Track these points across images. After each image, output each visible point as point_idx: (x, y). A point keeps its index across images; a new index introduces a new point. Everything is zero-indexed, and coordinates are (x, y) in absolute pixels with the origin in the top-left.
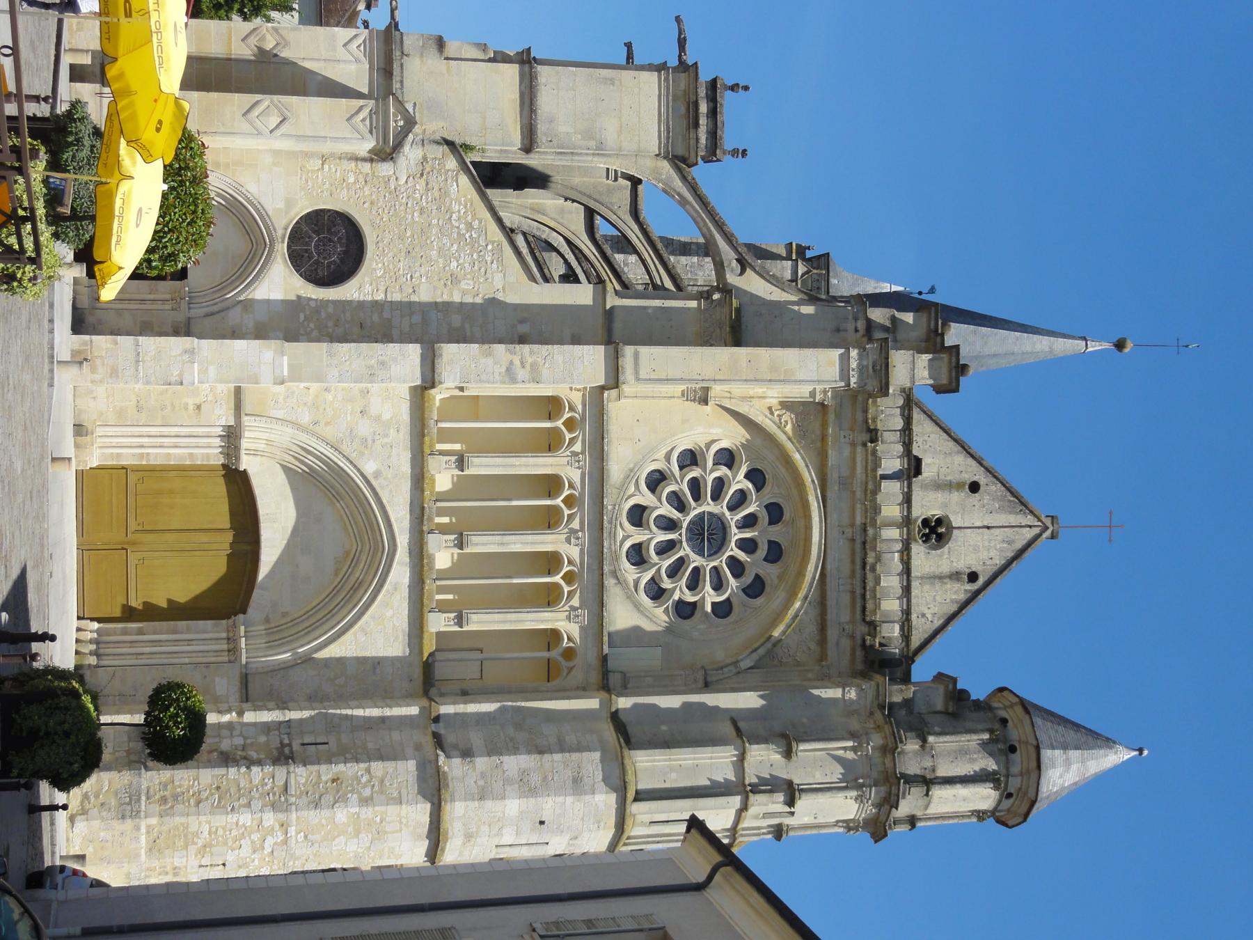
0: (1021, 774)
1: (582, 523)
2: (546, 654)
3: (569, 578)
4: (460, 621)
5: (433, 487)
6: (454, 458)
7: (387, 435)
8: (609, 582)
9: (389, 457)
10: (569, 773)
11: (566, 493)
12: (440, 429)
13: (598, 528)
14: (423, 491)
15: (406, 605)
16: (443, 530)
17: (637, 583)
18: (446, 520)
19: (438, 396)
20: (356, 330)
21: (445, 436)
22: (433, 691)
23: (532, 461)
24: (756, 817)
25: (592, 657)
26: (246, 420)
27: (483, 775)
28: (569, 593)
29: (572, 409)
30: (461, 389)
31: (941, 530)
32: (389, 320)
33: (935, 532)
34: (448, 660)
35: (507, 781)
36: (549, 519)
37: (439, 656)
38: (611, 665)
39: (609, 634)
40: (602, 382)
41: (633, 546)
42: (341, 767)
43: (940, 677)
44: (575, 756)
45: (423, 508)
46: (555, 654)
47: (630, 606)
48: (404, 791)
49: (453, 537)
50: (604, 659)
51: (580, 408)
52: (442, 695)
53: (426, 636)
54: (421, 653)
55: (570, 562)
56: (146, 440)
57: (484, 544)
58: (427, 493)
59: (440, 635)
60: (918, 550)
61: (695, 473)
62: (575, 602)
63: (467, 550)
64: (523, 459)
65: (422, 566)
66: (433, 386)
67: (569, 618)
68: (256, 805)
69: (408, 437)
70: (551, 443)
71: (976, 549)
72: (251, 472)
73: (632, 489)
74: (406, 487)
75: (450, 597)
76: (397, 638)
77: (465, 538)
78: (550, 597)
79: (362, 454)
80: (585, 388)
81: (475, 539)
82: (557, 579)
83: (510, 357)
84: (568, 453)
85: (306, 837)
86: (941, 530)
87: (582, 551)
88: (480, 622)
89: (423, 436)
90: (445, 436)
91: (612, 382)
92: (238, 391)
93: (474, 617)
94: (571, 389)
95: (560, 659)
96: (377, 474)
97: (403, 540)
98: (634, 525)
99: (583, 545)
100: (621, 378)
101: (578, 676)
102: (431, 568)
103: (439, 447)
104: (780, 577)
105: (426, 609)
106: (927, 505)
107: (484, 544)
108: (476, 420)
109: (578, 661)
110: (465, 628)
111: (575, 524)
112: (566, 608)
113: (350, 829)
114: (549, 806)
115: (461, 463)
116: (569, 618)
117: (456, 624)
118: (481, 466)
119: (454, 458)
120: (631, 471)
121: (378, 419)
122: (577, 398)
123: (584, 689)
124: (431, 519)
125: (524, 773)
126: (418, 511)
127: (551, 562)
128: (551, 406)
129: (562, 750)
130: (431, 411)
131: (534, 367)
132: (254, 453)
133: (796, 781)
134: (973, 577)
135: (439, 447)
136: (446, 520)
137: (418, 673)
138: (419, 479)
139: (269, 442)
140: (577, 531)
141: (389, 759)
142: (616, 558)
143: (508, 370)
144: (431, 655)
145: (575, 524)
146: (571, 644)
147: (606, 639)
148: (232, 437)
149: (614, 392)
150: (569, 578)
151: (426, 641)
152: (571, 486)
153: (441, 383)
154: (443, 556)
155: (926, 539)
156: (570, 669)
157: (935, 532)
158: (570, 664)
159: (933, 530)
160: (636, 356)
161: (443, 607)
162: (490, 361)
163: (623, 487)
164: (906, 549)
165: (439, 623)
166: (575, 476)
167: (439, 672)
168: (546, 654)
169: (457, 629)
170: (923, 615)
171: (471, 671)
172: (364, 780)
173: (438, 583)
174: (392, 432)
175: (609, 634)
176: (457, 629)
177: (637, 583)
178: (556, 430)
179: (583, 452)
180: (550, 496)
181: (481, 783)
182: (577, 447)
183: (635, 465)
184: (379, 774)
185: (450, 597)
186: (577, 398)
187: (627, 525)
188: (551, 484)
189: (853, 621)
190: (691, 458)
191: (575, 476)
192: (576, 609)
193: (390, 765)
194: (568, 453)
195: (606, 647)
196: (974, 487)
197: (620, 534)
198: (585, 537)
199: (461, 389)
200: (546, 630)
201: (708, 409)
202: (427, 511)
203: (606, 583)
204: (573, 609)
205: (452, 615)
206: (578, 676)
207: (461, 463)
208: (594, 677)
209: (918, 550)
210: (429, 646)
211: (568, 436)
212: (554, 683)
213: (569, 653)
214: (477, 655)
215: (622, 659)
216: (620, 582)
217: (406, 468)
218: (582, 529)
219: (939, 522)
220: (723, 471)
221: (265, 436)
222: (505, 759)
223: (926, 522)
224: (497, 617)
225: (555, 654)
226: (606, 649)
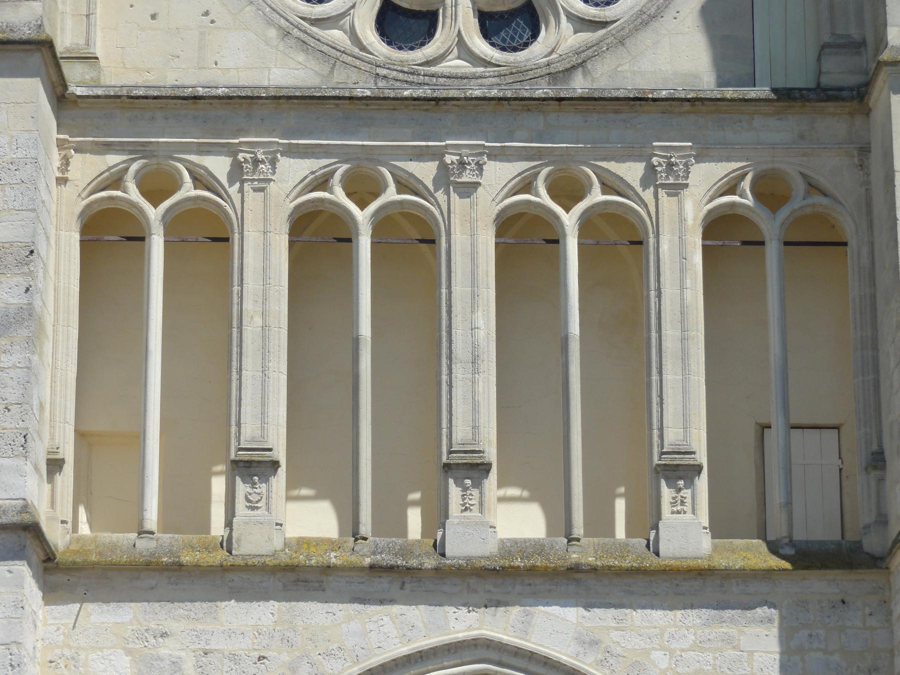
1: (420, 155)
2: (772, 250)
3: (568, 191)
4: (680, 472)
5: (319, 542)
6: (242, 488)
8: (579, 85)
9: (234, 657)
11: (339, 195)
12: (166, 525)
13: (435, 109)
14: (328, 569)
15: (637, 617)
16: (437, 516)
17: (583, 24)
18: (414, 519)
19: (67, 525)
21: (186, 507)
22: (872, 544)
23: (252, 284)
25: (779, 130)
28: (607, 188)
29: (116, 181)
30: (55, 465)
34: (788, 504)
36: (412, 242)
37: (777, 530)
38: (800, 79)
39: (719, 85)
40: (31, 90)
41: (486, 34)
45: (372, 567)
46: (771, 228)
47: (646, 38)
49: (455, 492)
50: (786, 96)
51: (113, 159)
52: (882, 520)
53: (721, 562)
54: (768, 574)
55: (527, 186)
57: (474, 411)
58: (334, 558)
59: (720, 527)
62: (631, 172)
63: (491, 454)
64: (248, 305)
65: (532, 571)
66: (33, 530)
67: (676, 189)
69: (181, 609)
70: (206, 237)
73: (336, 35)
74: (314, 614)
75: (620, 505)
76: (728, 641)
77: (456, 459)
78: (620, 243)
80: (61, 144)
81: (461, 433)
82: (570, 220)
84: (233, 190)
87: (496, 155)
88: (685, 416)
89: (178, 567)
90: (186, 507)
91: (36, 59)
93: (673, 436)
94: (62, 181)
95: (784, 212)
97: (461, 623)
98: (430, 34)
99: (480, 151)
100: (26, 33)
101: (831, 167)
102: (538, 547)
103: (218, 528)
105: (651, 561)
107: (474, 411)
108: (140, 437)
109: (790, 166)
110: (702, 458)
111: (425, 171)
112: (648, 195)
115: (253, 467)
116: (676, 189)
117: (690, 484)
118: (264, 413)
119: (242, 488)
120: (287, 34)
122: (88, 167)
123: (865, 150)
124: (407, 550)
126: (383, 583)
127: (524, 239)
128: (108, 236)
130: (113, 547)
135: (218, 528)
136: (414, 519)
137: (821, 585)
138: (296, 578)
140: (444, 168)
142: (519, 73)
144: (774, 549)
145: (425, 171)
146: (746, 184)
147: (730, 92)
149: (74, 73)
150: (568, 191)
151: (736, 562)
152: (322, 182)
153: (25, 508)
154: (513, 521)
156: (813, 187)
158: (800, 186)
161: (646, 519)
163: (331, 56)
165: (687, 530)
166: (293, 172)
167: (818, 526)
168: (772, 250)
169: (702, 483)
171: (817, 454)
173: (578, 530)
174: (167, 649)
175: (722, 82)
176: (702, 483)
177: (583, 24)
178: (171, 223)
179: (232, 151)
180: (348, 240)
182: (219, 166)
183: (270, 23)
185: (620, 505)
186: (88, 167)
187: (430, 50)
188: (316, 237)
191: (293, 172)
192: (651, 169)
194: (233, 190)
195: (752, 93)
197: (455, 64)
198: (457, 145)
199: (55, 465)
200: (707, 251)
202: (386, 559)
203: (579, 92)
204: (649, 178)
205: (667, 493)
206: (831, 167)
207: (253, 467)
208: (832, 124)
210: (752, 554)
211: (188, 190)
212: (848, 228)
213: (770, 191)
214: (775, 438)
215: (786, 50)
216: (580, 63)
217: (265, 613)
218: (437, 155)
224: (671, 376)
225: (771, 228)
226: (762, 91)
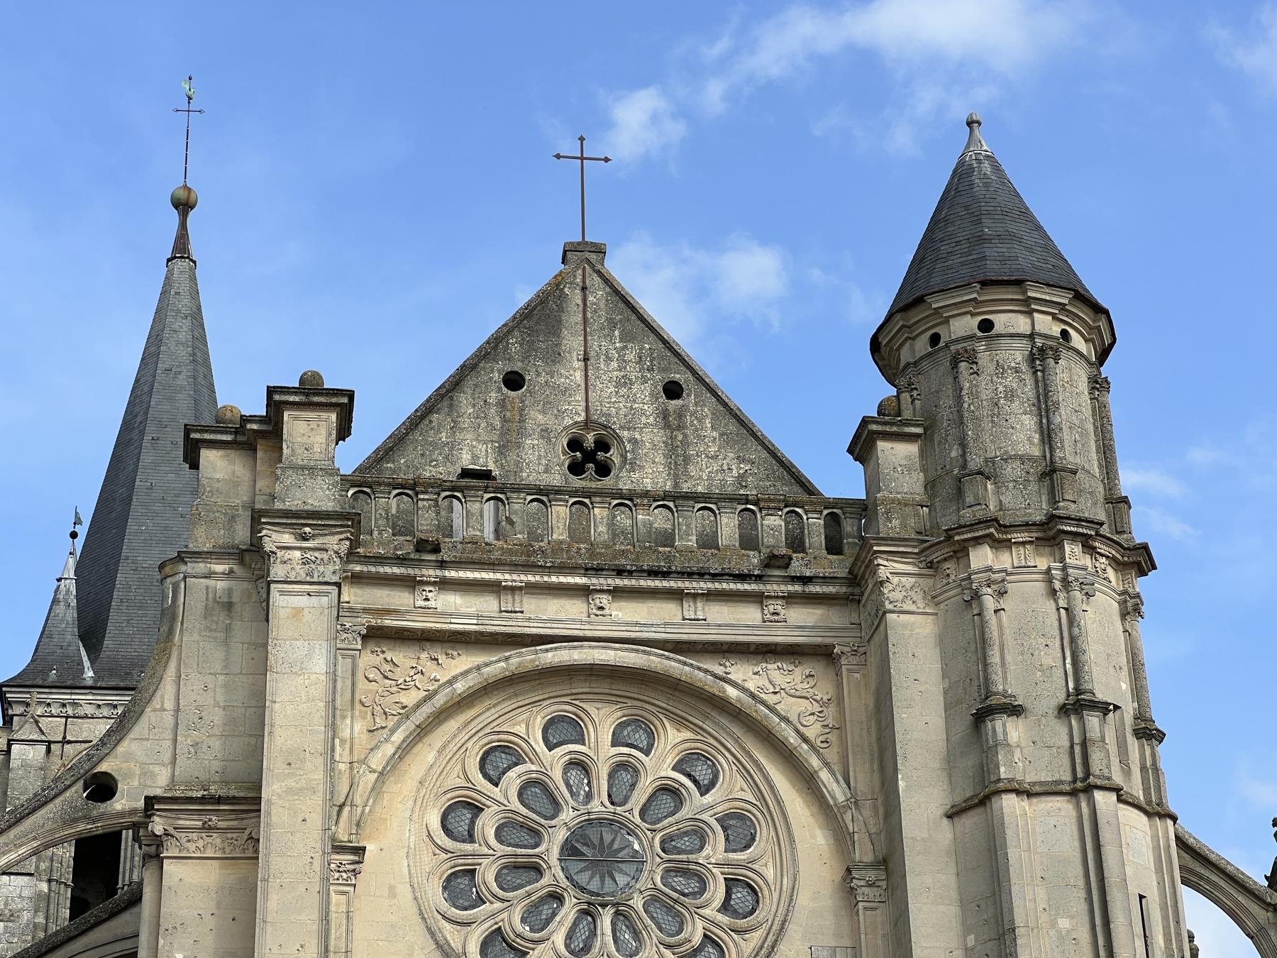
104: (681, 722)
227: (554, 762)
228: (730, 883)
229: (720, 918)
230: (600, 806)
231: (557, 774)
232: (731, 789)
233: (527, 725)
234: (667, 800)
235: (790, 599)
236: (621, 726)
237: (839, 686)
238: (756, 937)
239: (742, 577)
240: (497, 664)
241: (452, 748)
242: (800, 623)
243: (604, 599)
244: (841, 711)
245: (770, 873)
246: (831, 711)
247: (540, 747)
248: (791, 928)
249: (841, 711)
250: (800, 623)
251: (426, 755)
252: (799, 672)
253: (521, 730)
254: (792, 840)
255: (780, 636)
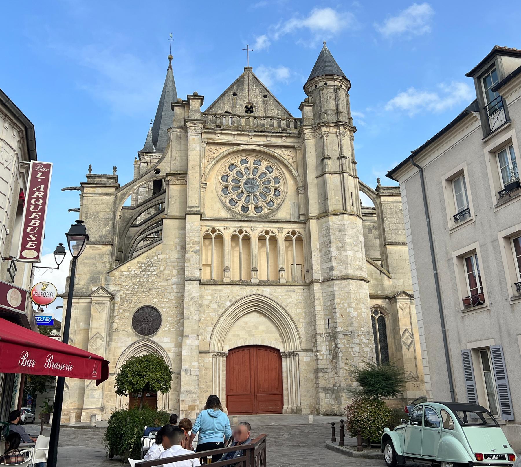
0: (334, 81)
7: (217, 298)
10: (337, 233)
20: (178, 309)
24: (350, 170)
26: (211, 349)
27: (339, 263)
31: (249, 106)
32: (175, 296)
33: (249, 109)
35: (341, 254)
42: (337, 314)
43: (301, 108)
44: (331, 231)
48: (346, 291)
56: (217, 388)
60: (256, 114)
61: (230, 188)
68: (352, 345)
71: (256, 95)
72: (229, 349)
79: (223, 307)
83: (190, 252)
85: (362, 327)
86: (249, 106)
92: (200, 352)
96: (230, 301)
104: (266, 160)
106: (240, 110)
113: (359, 311)
114: (349, 241)
121: (211, 301)
125: (338, 249)
129: (329, 235)
131: (193, 243)
132: (222, 347)
133: (338, 156)
134: (265, 97)
139: (219, 342)
141: (334, 297)
143: (195, 253)
148: (217, 354)
155: (252, 112)
157: (249, 109)
159: (249, 109)
160: (189, 207)
162: (192, 259)
164: (257, 118)
170: (278, 113)
172: (342, 306)
181: (341, 264)
184: (339, 300)
187: (248, 213)
189: (281, 137)
190: (225, 190)
193: (336, 296)
196: (235, 94)
201: (208, 183)
209: (256, 114)
219: (246, 107)
220: (230, 179)
221: (216, 343)
222: (333, 255)
223: (247, 112)
227: (242, 168)
228: (275, 190)
229: (273, 196)
230: (251, 176)
231: (243, 170)
232: (275, 173)
233: (237, 160)
234: (264, 175)
235: (287, 137)
236: (255, 161)
237: (296, 153)
238: (280, 200)
239: (278, 133)
240: (232, 149)
241: (223, 165)
242: (289, 141)
243: (252, 137)
244: (296, 158)
245: (283, 188)
246: (295, 158)
247: (240, 165)
248: (286, 198)
249: (296, 158)
250: (289, 141)
251: (218, 166)
252: (289, 151)
253: (236, 161)
254: (287, 182)
255: (285, 144)
